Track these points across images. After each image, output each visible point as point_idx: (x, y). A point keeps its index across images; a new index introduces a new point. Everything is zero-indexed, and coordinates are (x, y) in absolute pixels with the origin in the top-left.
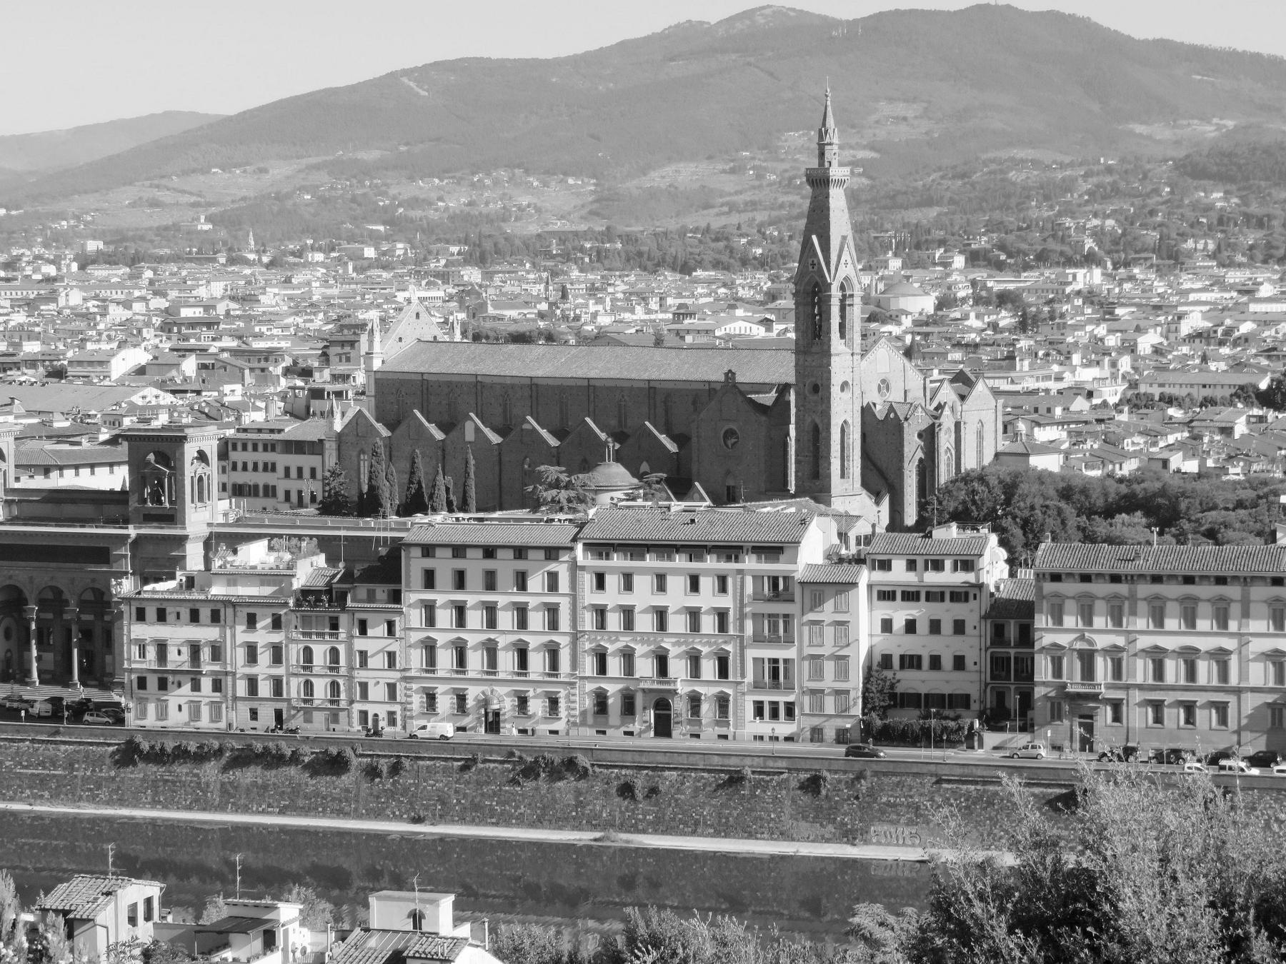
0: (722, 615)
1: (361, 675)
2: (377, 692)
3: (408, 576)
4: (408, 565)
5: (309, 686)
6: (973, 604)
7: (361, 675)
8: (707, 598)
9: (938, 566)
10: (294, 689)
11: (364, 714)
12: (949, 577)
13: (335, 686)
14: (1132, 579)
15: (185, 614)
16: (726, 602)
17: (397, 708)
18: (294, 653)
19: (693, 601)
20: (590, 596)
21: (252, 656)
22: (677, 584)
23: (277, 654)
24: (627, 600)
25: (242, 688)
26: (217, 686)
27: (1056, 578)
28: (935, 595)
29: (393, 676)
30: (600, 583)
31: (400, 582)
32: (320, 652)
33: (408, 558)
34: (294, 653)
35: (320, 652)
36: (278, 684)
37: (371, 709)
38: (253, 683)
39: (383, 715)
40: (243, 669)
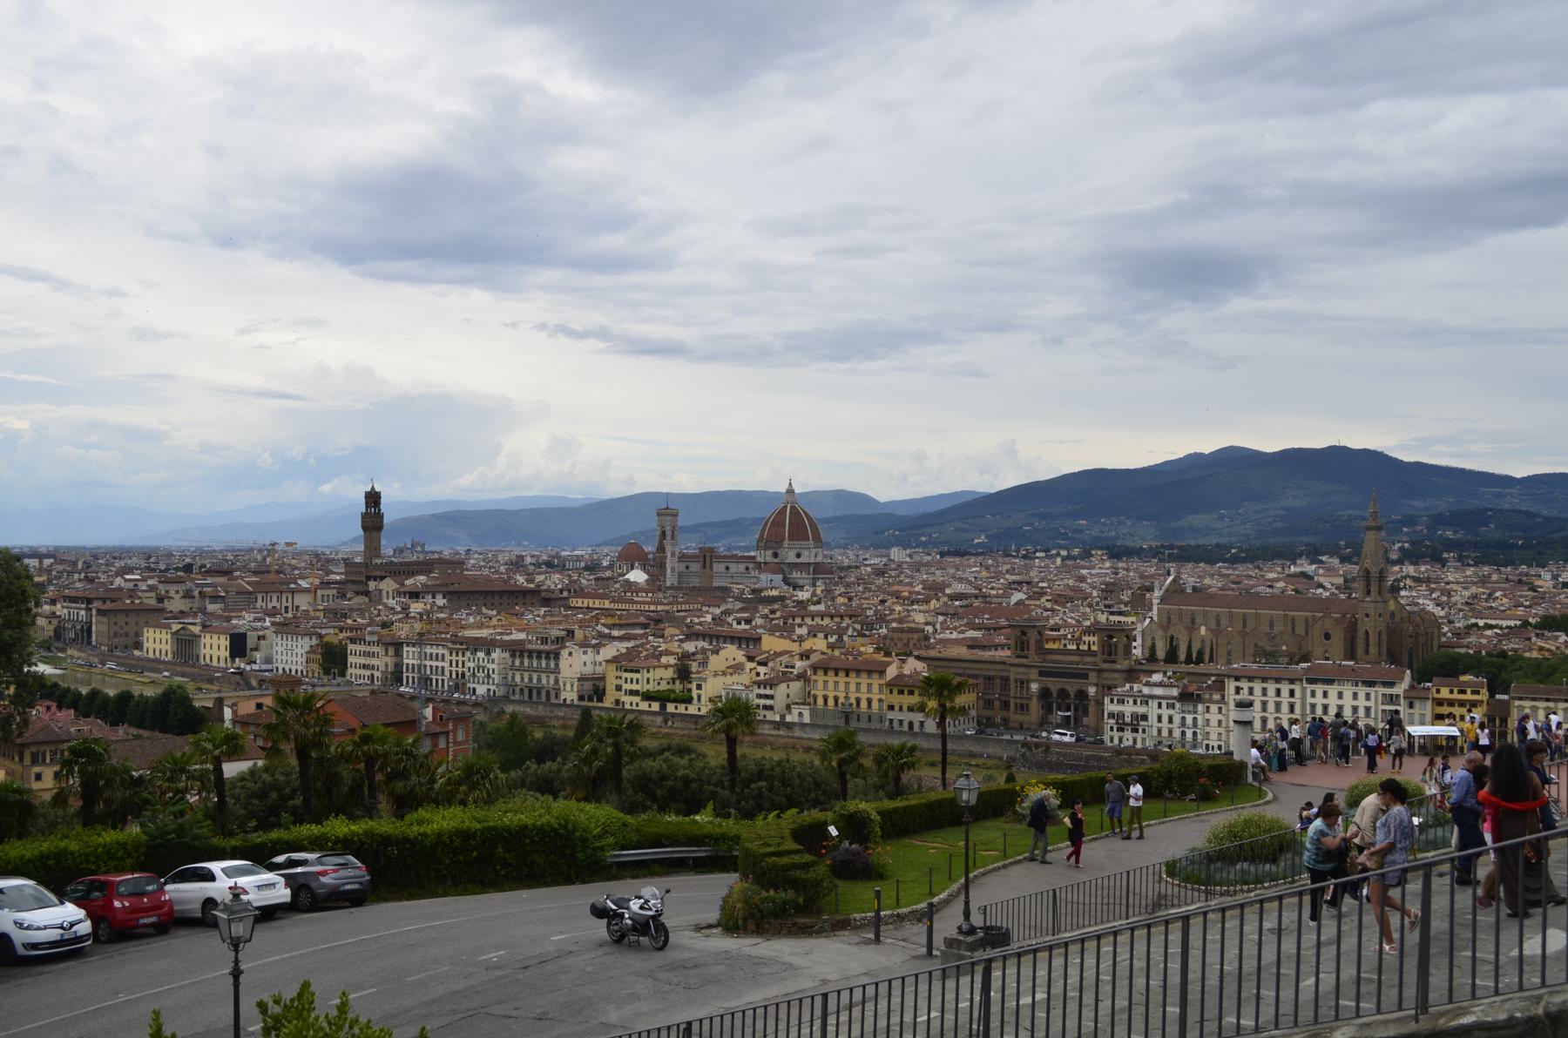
0: (1368, 709)
1: (1207, 729)
2: (1214, 736)
5: (1183, 733)
6: (1479, 709)
7: (1207, 729)
8: (1361, 702)
9: (1463, 692)
10: (1177, 734)
11: (1207, 746)
12: (1469, 696)
13: (1195, 734)
14: (1556, 701)
15: (1131, 701)
16: (1371, 704)
17: (1222, 743)
18: (1177, 720)
19: (1355, 703)
20: (1310, 700)
21: (1160, 719)
22: (1348, 694)
23: (1171, 720)
24: (1325, 701)
25: (1155, 733)
26: (1144, 731)
27: (1521, 699)
28: (1462, 704)
29: (1221, 730)
30: (1313, 694)
32: (1189, 721)
34: (1177, 720)
35: (1189, 721)
36: (1170, 732)
37: (1211, 743)
38: (1159, 731)
39: (1216, 746)
40: (1156, 724)
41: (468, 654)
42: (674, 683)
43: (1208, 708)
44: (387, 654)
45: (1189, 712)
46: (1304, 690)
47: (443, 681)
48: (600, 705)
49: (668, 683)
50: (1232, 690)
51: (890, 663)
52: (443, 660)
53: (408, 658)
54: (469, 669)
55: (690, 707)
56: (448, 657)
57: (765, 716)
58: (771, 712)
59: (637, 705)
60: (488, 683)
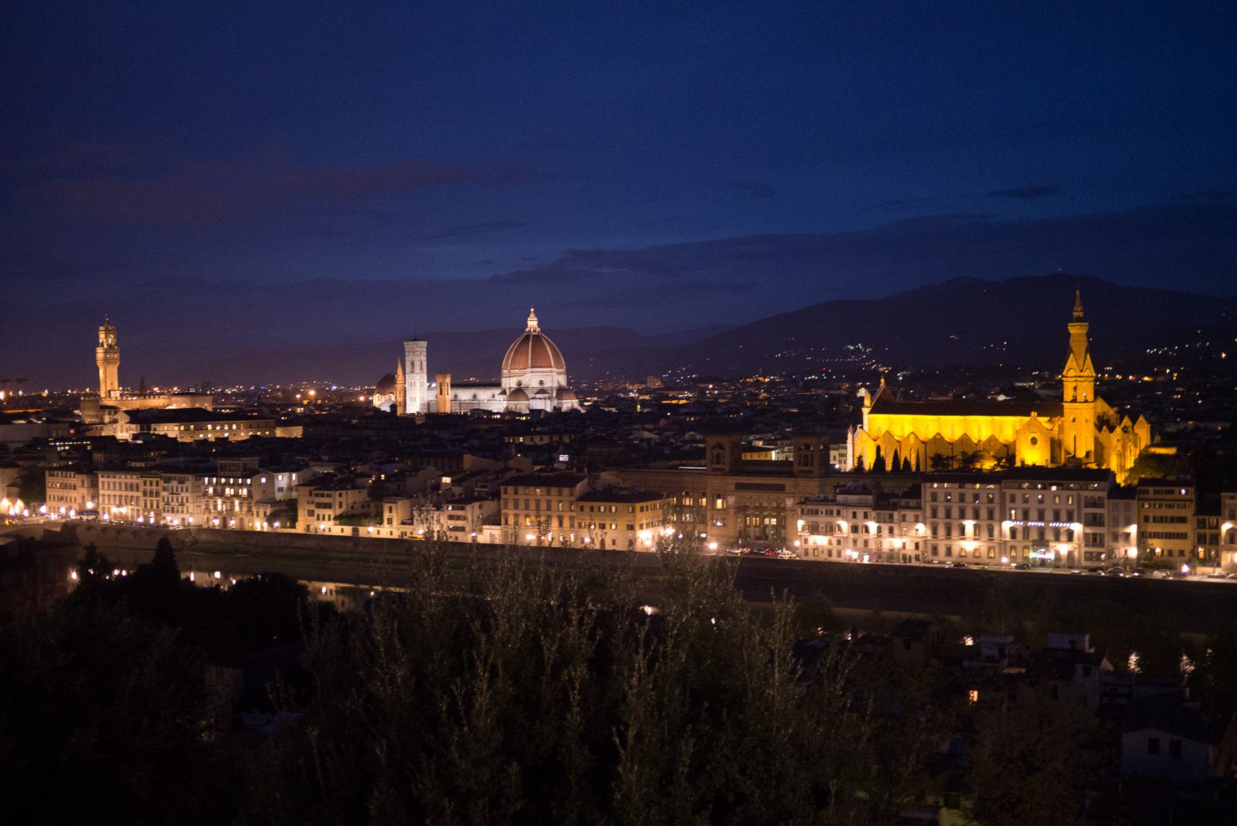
3: (925, 496)
4: (925, 492)
31: (920, 498)
33: (925, 488)
41: (162, 483)
42: (369, 506)
43: (904, 516)
44: (83, 486)
45: (885, 522)
46: (1003, 495)
47: (138, 510)
48: (293, 531)
49: (363, 507)
50: (928, 498)
51: (581, 479)
52: (137, 490)
53: (103, 488)
54: (163, 498)
55: (381, 530)
56: (142, 487)
57: (457, 538)
58: (463, 533)
59: (330, 530)
60: (182, 512)
